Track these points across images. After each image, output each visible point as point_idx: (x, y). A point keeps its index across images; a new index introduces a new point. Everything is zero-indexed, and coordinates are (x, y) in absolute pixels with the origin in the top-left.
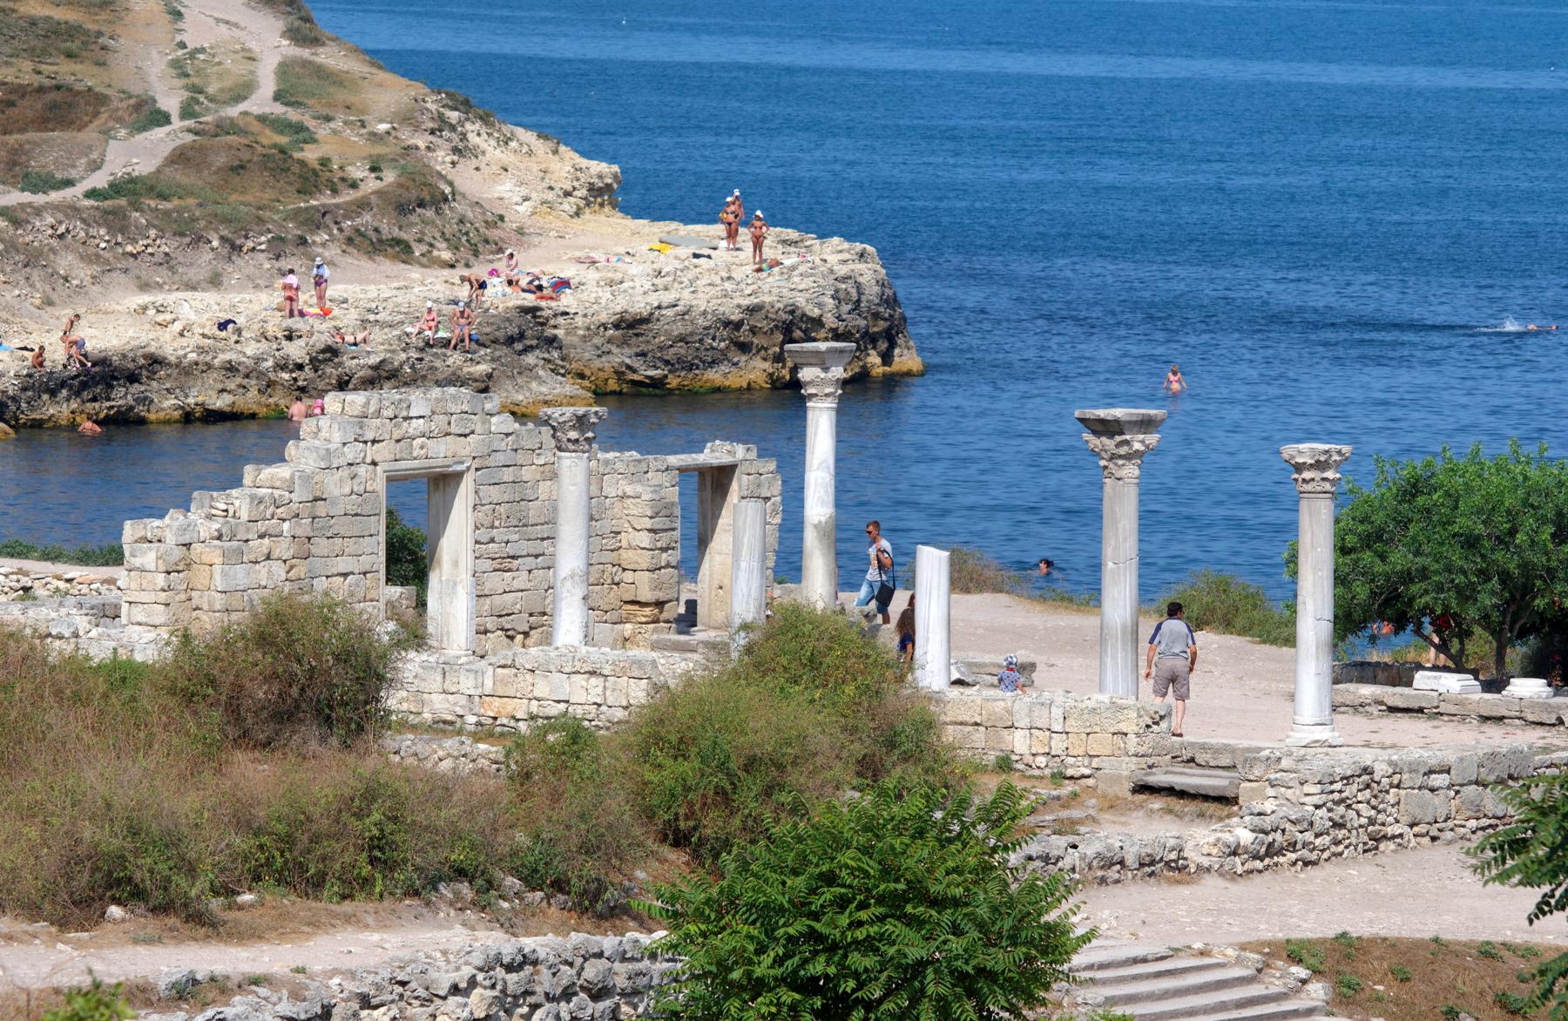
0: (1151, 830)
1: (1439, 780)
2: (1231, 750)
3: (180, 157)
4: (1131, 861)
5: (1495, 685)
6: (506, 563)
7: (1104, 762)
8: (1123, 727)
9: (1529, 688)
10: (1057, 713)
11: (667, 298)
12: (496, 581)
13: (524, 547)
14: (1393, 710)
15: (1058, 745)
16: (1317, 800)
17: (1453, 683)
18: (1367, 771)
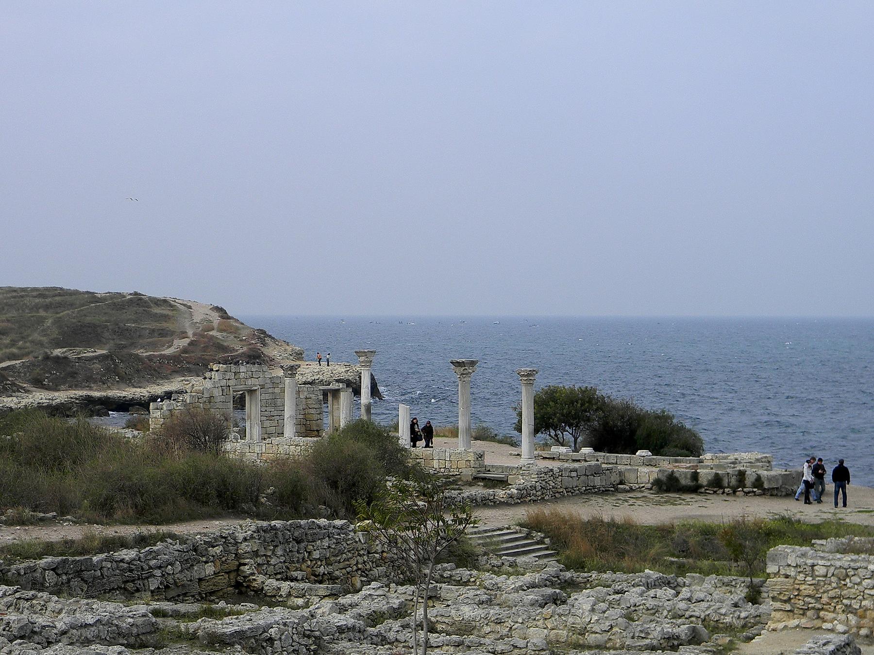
0: (478, 491)
1: (574, 474)
2: (502, 467)
3: (191, 343)
4: (479, 500)
5: (576, 450)
6: (270, 418)
7: (463, 470)
8: (469, 458)
9: (587, 450)
10: (447, 454)
11: (316, 378)
12: (267, 424)
13: (276, 413)
14: (545, 458)
15: (448, 465)
16: (536, 480)
17: (563, 450)
18: (552, 470)
